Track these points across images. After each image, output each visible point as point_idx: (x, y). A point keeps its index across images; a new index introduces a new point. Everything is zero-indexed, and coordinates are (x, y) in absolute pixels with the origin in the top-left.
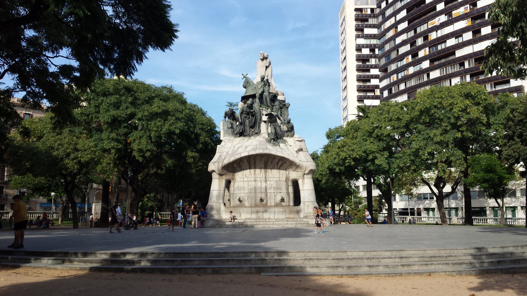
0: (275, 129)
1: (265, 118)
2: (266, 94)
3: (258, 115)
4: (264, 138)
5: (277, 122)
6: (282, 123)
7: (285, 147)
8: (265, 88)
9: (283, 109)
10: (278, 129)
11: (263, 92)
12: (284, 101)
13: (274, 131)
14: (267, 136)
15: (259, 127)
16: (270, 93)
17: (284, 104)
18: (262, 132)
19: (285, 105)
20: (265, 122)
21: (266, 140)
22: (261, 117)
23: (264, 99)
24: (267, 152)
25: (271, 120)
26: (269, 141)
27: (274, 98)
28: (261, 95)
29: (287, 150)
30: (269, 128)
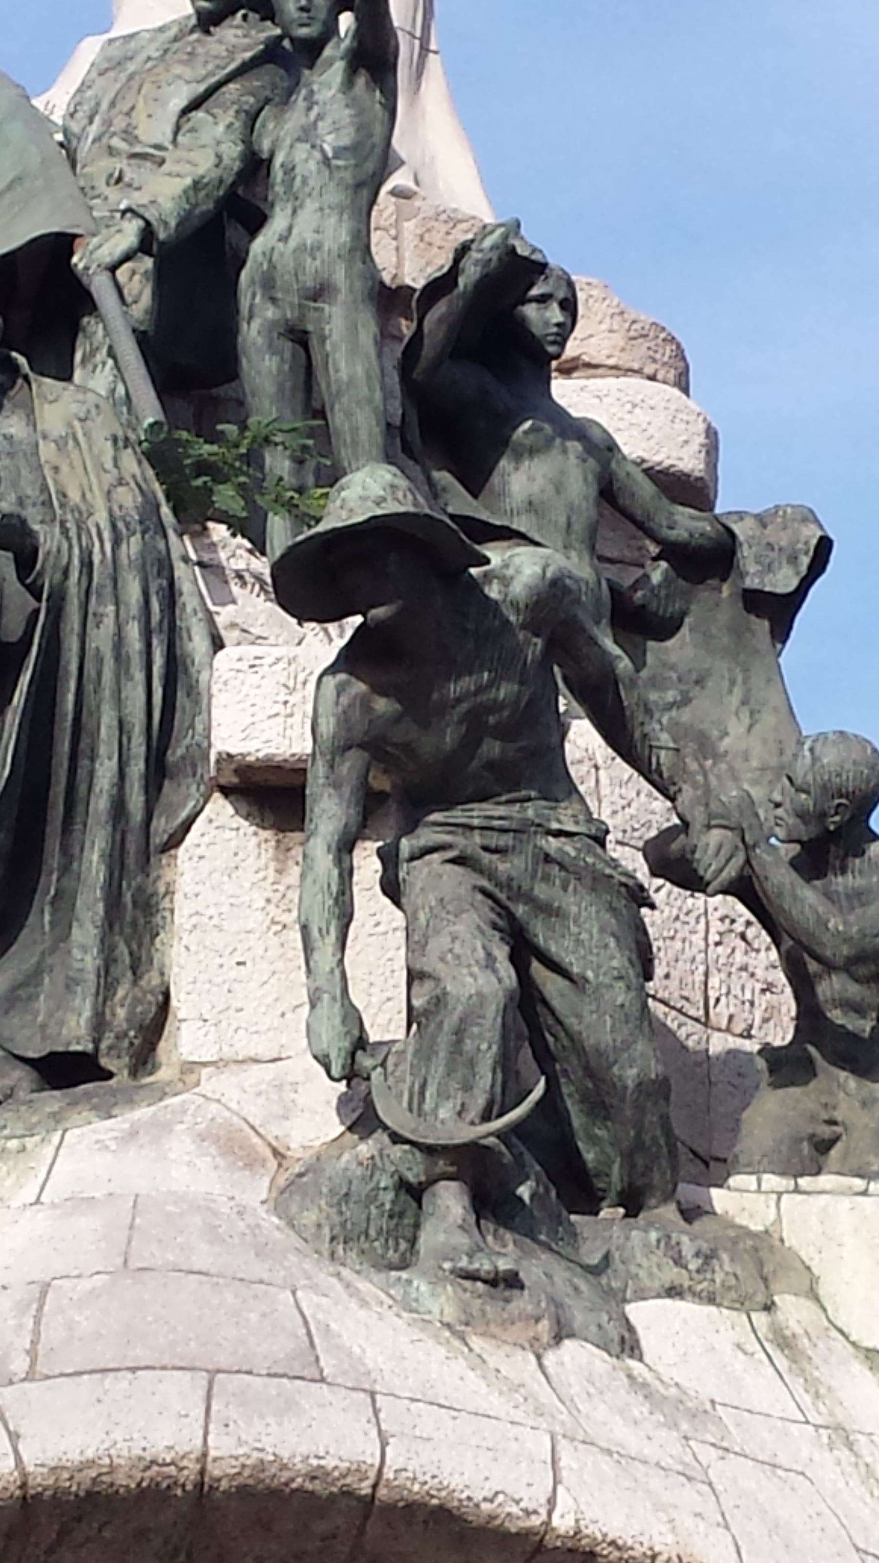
0: (523, 950)
1: (270, 682)
2: (297, 233)
3: (108, 630)
4: (236, 1146)
5: (553, 779)
6: (674, 862)
7: (761, 1385)
8: (280, 135)
9: (678, 650)
10: (582, 938)
11: (240, 201)
12: (692, 491)
13: (479, 978)
14: (313, 1116)
15: (135, 916)
16: (388, 299)
17: (685, 523)
18: (187, 1039)
19: (710, 559)
20: (271, 795)
21: (282, 1200)
22: (176, 685)
23: (262, 366)
24: (313, 1437)
25: (418, 706)
26: (378, 1228)
27: (483, 349)
28: (201, 255)
29: (803, 1446)
30: (375, 915)
